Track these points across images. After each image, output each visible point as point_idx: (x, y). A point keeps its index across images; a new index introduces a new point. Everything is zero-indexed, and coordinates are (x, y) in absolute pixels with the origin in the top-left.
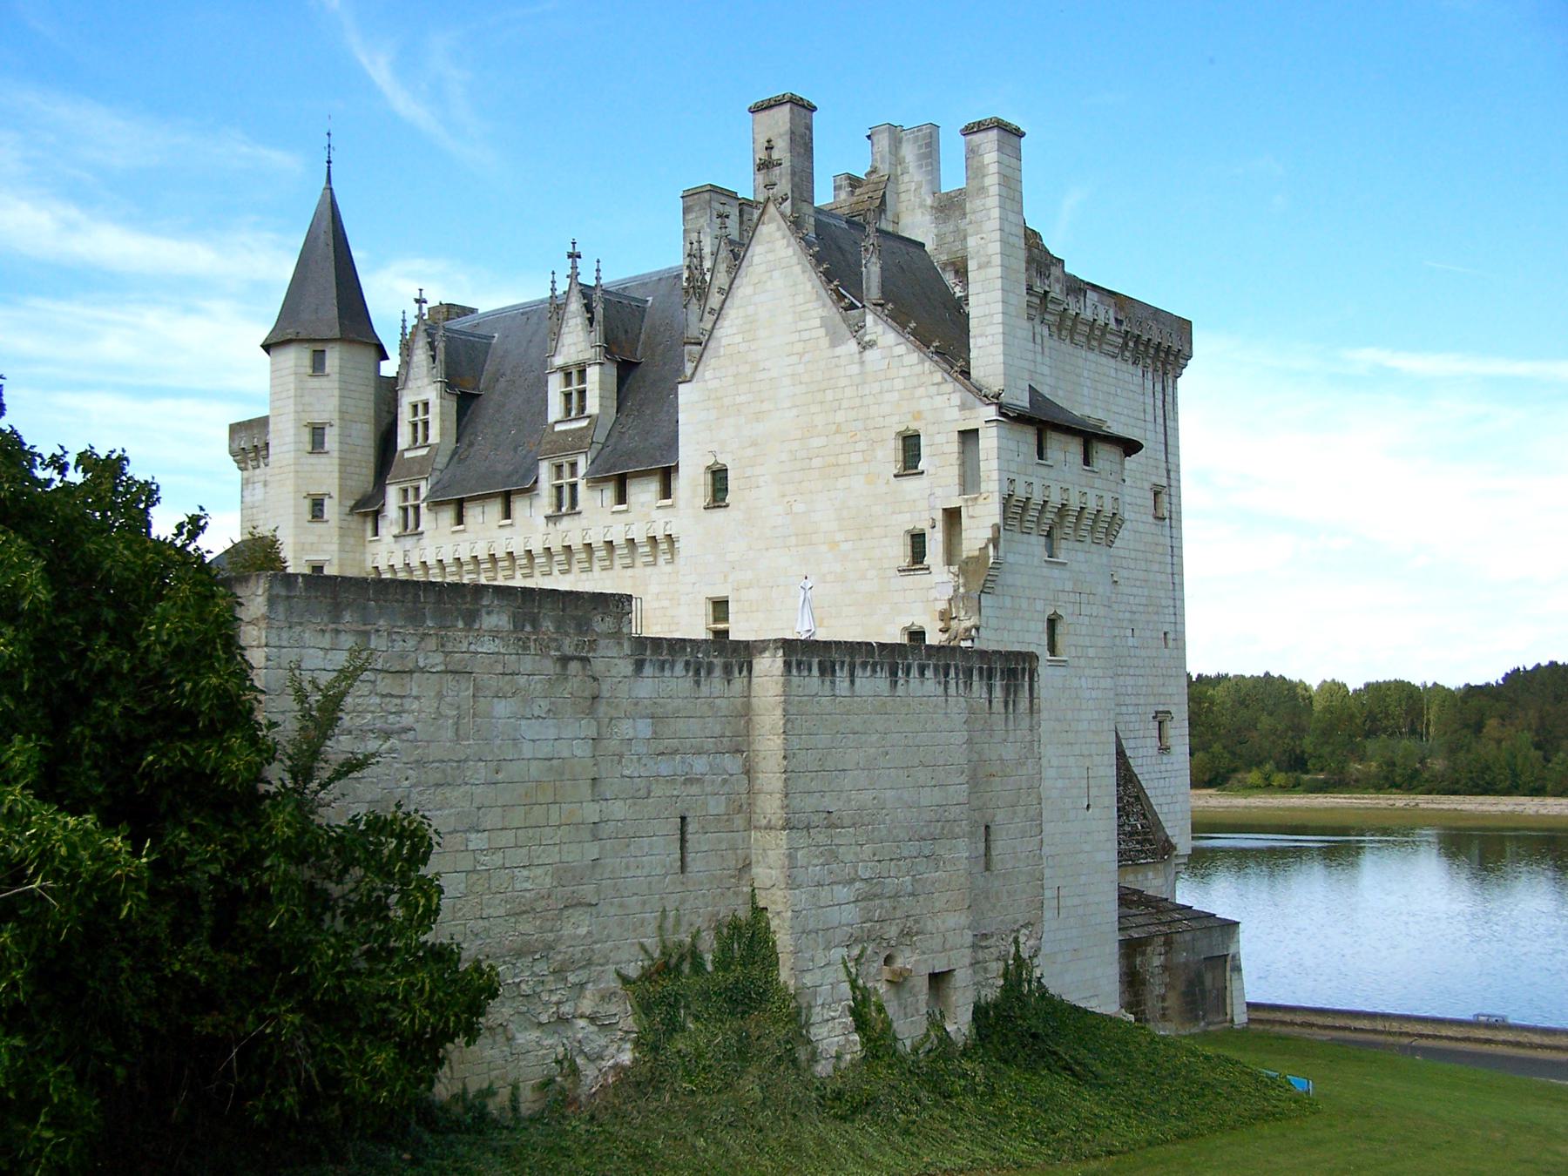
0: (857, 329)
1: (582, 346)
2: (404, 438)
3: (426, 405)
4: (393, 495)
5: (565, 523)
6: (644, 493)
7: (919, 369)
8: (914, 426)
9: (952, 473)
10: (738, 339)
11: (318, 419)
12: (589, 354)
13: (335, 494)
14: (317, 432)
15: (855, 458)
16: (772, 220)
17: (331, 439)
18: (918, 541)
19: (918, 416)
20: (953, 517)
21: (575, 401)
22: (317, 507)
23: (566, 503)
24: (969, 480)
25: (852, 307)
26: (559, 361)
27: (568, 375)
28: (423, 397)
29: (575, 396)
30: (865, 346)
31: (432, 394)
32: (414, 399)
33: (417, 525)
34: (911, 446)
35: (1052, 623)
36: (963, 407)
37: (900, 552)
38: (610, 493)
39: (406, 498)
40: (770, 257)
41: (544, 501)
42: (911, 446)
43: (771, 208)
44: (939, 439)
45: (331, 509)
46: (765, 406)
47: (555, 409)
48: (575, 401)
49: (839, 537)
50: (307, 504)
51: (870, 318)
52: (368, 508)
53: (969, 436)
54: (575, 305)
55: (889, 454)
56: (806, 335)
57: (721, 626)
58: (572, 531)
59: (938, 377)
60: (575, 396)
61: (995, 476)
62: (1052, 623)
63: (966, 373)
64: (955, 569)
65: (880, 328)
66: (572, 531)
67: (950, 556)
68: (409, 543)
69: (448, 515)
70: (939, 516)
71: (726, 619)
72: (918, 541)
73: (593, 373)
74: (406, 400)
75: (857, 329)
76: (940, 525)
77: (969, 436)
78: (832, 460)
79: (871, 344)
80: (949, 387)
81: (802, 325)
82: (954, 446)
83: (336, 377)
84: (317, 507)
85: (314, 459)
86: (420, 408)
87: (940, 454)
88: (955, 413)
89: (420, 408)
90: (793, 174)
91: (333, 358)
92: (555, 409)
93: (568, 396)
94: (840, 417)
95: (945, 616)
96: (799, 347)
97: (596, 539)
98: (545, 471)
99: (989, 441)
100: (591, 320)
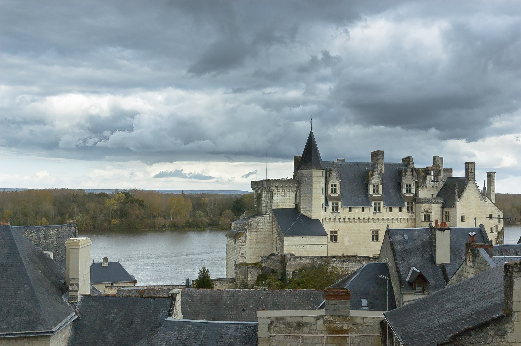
3: (335, 186)
5: (378, 214)
6: (396, 210)
20: (497, 225)
21: (376, 191)
23: (377, 210)
27: (374, 186)
28: (336, 183)
30: (485, 201)
32: (332, 183)
38: (388, 209)
41: (373, 208)
48: (376, 191)
66: (378, 215)
67: (497, 231)
68: (335, 214)
69: (347, 210)
75: (484, 199)
97: (386, 217)
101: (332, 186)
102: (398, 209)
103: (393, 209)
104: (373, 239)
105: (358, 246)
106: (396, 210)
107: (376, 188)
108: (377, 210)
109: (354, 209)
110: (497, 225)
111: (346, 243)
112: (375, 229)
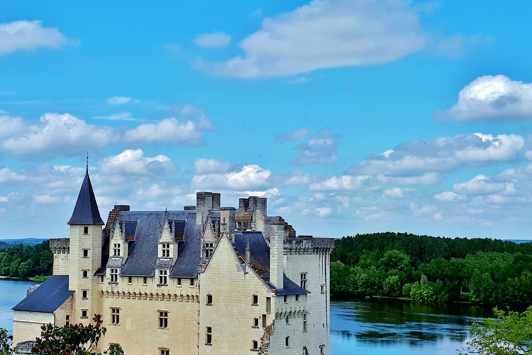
0: (244, 269)
1: (168, 238)
2: (111, 253)
3: (119, 245)
4: (108, 271)
6: (186, 283)
7: (258, 281)
8: (256, 294)
9: (264, 307)
10: (215, 265)
11: (86, 248)
12: (171, 241)
13: (91, 270)
14: (86, 253)
15: (243, 299)
16: (224, 238)
17: (89, 254)
18: (256, 321)
19: (257, 292)
20: (264, 316)
21: (166, 253)
22: (85, 274)
23: (163, 282)
24: (268, 309)
25: (244, 262)
26: (161, 241)
27: (164, 246)
28: (119, 243)
29: (166, 252)
31: (121, 242)
32: (115, 243)
33: (116, 280)
34: (256, 298)
35: (287, 339)
36: (267, 292)
37: (253, 323)
38: (176, 281)
39: (112, 272)
40: (224, 247)
42: (256, 298)
43: (224, 235)
44: (261, 298)
45: (89, 274)
46: (222, 283)
47: (160, 254)
48: (166, 253)
49: (238, 317)
50: (82, 273)
51: (247, 267)
52: (100, 272)
53: (268, 299)
54: (167, 226)
55: (251, 300)
56: (232, 268)
57: (209, 334)
58: (164, 290)
59: (262, 284)
60: (166, 252)
61: (274, 309)
62: (287, 339)
63: (268, 279)
64: (264, 328)
65: (249, 270)
66: (164, 290)
68: (114, 285)
69: (126, 279)
70: (261, 316)
71: (211, 332)
72: (256, 321)
73: (171, 246)
74: (112, 243)
76: (261, 318)
77: (268, 299)
78: (237, 298)
79: (247, 273)
80: (264, 286)
81: (231, 265)
82: (265, 301)
83: (91, 235)
84: (85, 274)
85: (84, 259)
86: (117, 245)
87: (262, 301)
88: (266, 293)
89: (117, 245)
90: (230, 227)
91: (90, 229)
92: (160, 254)
93: (164, 251)
94: (239, 289)
95: (262, 339)
96: (230, 270)
97: (172, 293)
98: (157, 272)
99: (273, 300)
100: (171, 231)
101: (115, 245)
102: (189, 281)
103: (183, 281)
104: (161, 325)
105: (141, 332)
106: (186, 283)
107: (166, 249)
108: (163, 282)
109: (134, 280)
110: (264, 316)
111: (128, 327)
112: (163, 309)
